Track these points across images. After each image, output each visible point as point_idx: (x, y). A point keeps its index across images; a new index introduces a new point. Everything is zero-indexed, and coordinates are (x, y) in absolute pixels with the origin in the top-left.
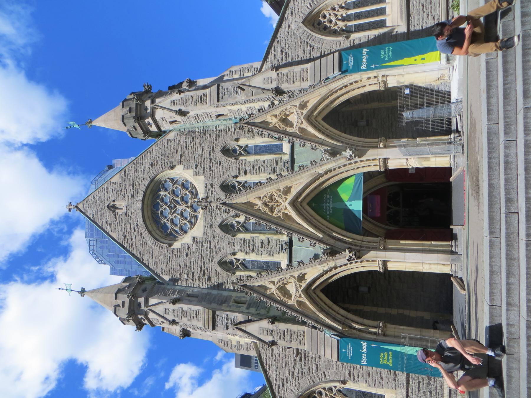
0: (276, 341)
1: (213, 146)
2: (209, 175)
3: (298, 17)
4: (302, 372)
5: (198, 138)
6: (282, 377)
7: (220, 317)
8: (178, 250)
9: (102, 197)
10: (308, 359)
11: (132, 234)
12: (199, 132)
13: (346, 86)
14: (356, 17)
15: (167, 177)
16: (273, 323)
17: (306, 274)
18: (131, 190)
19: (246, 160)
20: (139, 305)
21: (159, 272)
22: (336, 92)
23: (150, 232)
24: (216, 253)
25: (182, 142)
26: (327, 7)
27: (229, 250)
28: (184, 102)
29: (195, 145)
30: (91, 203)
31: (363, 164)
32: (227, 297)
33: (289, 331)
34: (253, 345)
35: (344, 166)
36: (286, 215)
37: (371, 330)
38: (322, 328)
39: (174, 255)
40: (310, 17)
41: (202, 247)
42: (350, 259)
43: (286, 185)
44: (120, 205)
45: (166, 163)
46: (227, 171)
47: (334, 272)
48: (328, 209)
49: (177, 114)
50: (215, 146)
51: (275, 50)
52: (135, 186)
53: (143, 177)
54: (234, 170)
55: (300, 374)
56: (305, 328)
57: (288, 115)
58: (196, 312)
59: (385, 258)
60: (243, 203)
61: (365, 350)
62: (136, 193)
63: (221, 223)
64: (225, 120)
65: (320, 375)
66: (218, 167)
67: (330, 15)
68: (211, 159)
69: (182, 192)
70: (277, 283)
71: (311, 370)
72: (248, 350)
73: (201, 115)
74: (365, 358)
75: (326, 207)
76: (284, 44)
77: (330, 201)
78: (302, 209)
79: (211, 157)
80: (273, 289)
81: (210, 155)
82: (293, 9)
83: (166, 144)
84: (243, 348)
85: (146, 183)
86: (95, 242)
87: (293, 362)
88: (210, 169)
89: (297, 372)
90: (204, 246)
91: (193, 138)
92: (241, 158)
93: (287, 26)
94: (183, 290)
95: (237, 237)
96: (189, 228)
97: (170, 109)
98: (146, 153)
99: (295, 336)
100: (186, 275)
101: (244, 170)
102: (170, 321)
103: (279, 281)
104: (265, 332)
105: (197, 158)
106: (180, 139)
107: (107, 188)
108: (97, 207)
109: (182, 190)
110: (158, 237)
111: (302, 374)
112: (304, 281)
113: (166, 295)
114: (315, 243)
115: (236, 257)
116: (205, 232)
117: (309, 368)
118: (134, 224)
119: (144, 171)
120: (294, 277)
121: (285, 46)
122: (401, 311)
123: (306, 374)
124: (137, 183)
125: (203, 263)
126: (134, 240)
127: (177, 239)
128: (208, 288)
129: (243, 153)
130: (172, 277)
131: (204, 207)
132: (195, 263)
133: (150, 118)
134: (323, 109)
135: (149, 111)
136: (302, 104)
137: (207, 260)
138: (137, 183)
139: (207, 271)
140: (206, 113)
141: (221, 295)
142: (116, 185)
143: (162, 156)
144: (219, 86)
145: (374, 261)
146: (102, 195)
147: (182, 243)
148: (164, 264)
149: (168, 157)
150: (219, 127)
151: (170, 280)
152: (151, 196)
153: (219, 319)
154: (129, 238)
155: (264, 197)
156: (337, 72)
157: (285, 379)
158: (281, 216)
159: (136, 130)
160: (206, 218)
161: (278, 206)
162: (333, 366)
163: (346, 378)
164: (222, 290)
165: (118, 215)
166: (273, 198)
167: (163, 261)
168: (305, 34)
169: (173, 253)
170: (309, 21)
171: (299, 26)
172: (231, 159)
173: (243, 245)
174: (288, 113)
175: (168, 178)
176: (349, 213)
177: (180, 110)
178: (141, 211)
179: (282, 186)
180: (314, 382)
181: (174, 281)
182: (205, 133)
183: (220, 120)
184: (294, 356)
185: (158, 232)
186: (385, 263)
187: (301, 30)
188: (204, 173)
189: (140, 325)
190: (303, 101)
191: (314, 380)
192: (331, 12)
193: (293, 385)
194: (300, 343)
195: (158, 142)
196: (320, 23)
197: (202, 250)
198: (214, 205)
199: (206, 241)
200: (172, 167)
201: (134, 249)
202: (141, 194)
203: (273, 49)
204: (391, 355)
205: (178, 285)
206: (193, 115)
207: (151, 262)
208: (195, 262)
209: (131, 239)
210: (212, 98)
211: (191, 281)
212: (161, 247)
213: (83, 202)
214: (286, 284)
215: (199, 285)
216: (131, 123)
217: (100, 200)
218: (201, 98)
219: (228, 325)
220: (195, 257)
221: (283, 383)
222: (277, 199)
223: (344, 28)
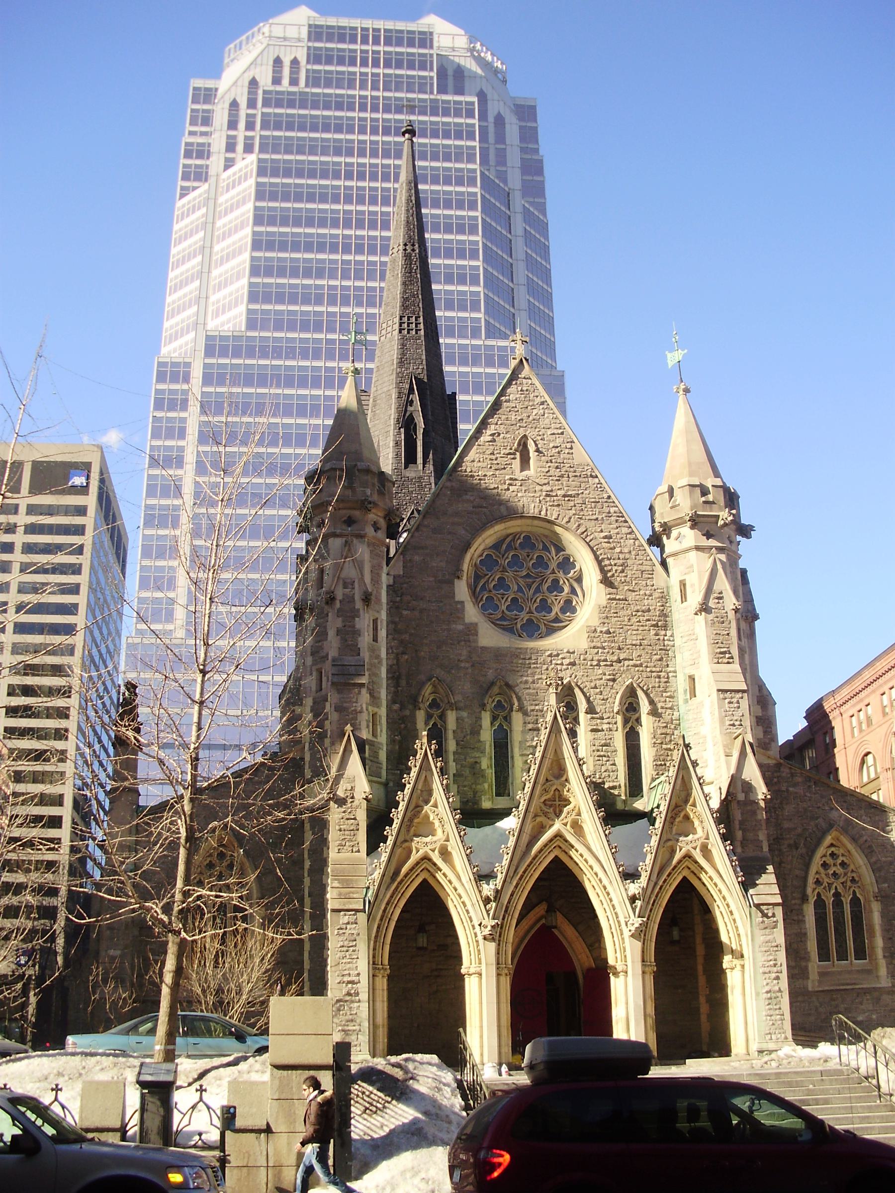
32: (379, 698)
126: (465, 497)
138: (572, 504)
140: (699, 656)
144: (743, 691)
147: (466, 604)
185: (482, 548)
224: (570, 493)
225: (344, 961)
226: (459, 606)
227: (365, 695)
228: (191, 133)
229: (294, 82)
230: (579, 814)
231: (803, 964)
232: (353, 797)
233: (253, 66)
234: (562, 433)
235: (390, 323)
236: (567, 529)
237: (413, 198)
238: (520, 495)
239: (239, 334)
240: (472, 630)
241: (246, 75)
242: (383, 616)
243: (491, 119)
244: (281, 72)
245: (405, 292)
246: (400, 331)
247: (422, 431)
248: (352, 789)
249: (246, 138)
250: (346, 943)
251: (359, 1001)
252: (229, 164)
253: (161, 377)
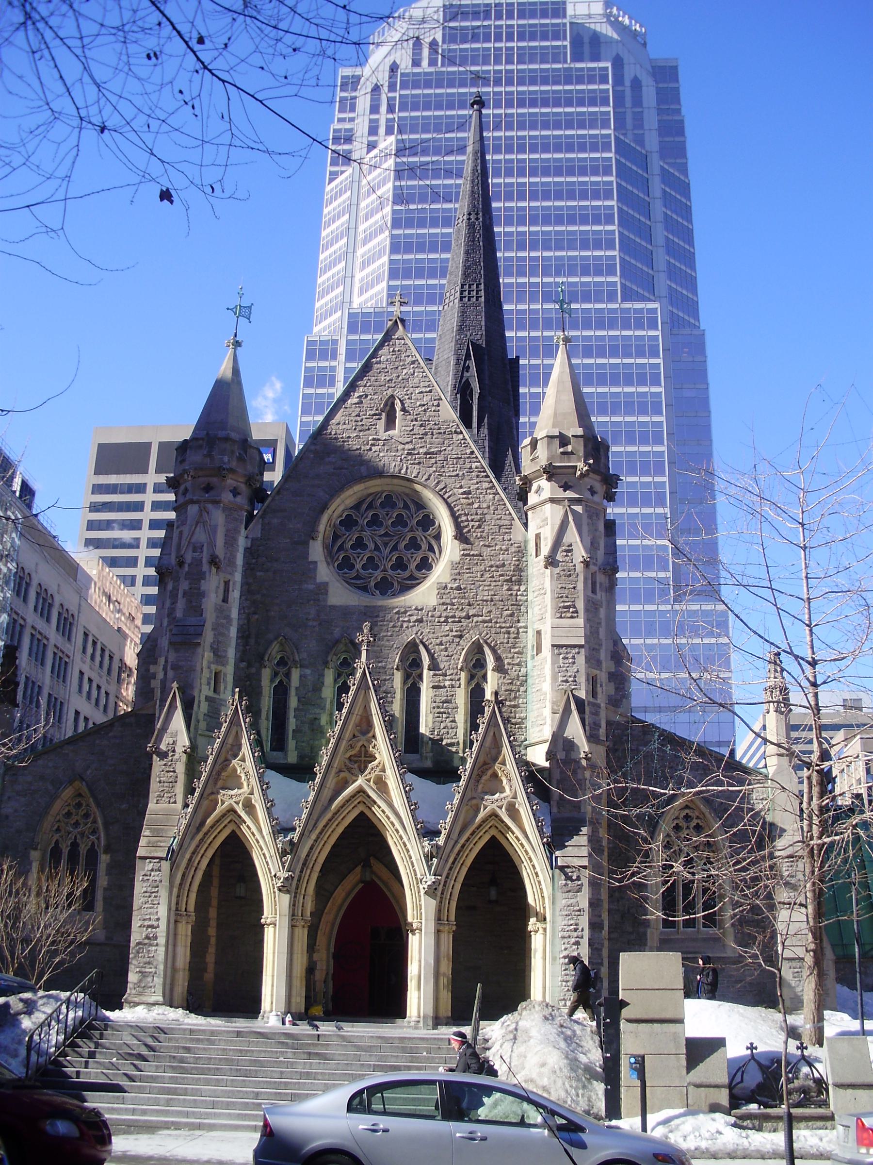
19: (459, 687)
32: (225, 657)
64: (533, 646)
78: (353, 805)
122: (213, 941)
126: (327, 460)
138: (433, 461)
142: (432, 414)
144: (581, 646)
159: (532, 460)
185: (341, 508)
188: (443, 604)
224: (432, 450)
225: (146, 906)
226: (311, 566)
227: (208, 655)
228: (340, 120)
229: (432, 62)
230: (384, 770)
231: (641, 930)
232: (174, 751)
233: (393, 51)
234: (430, 391)
235: (453, 291)
236: (425, 486)
237: (479, 168)
238: (381, 454)
239: (381, 310)
240: (323, 588)
241: (387, 60)
242: (238, 577)
243: (627, 83)
244: (420, 54)
245: (467, 260)
246: (461, 299)
247: (477, 395)
248: (174, 743)
249: (388, 120)
250: (149, 889)
251: (157, 945)
252: (371, 146)
253: (310, 356)
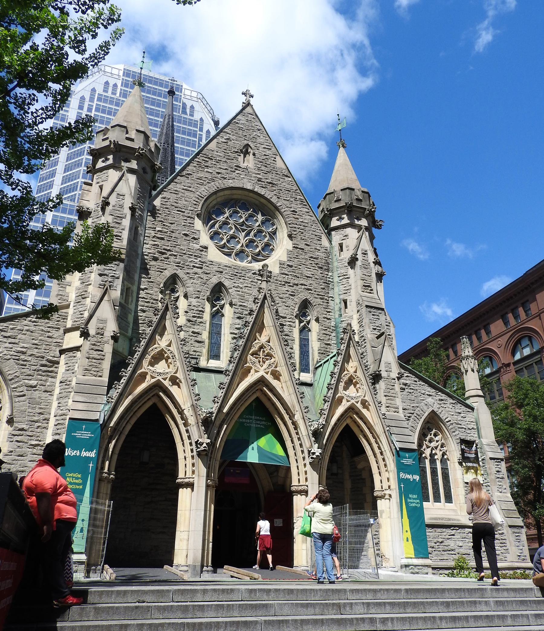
0: (89, 338)
1: (311, 290)
2: (280, 279)
3: (438, 406)
4: (26, 365)
5: (321, 273)
6: (18, 337)
7: (116, 267)
8: (193, 225)
9: (259, 140)
10: (43, 376)
11: (214, 169)
12: (328, 276)
13: (382, 453)
14: (433, 469)
15: (279, 227)
16: (113, 337)
17: (179, 387)
18: (266, 179)
19: (295, 327)
20: (127, 161)
21: (165, 194)
22: (377, 442)
23: (215, 193)
24: (188, 273)
25: (318, 254)
26: (445, 439)
27: (190, 290)
28: (365, 266)
29: (313, 268)
30: (253, 125)
31: (301, 467)
32: (133, 278)
33: (102, 357)
34: (65, 303)
35: (301, 445)
36: (248, 370)
37: (107, 463)
38: (113, 401)
39: (186, 218)
40: (437, 420)
41: (195, 256)
42: (199, 444)
43: (282, 375)
44: (248, 161)
45: (295, 229)
46: (284, 302)
47: (180, 422)
48: (248, 421)
49: (353, 256)
50: (312, 292)
51: (407, 376)
52: (271, 185)
53: (281, 198)
54: (284, 311)
55: (22, 363)
56: (105, 379)
57: (355, 386)
58: (120, 237)
59: (198, 487)
60: (263, 320)
61: (84, 454)
62: (263, 185)
63: (224, 286)
64: (340, 309)
65: (21, 389)
66: (288, 293)
67: (437, 441)
68: (297, 285)
69: (260, 243)
70: (169, 350)
71: (27, 377)
72: (58, 295)
73: (349, 283)
74: (73, 454)
75: (251, 419)
76: (413, 388)
77: (258, 424)
79: (300, 286)
80: (162, 343)
81: (302, 285)
82: (446, 402)
83: (316, 234)
84: (61, 289)
85: (274, 200)
86: (117, 77)
87: (40, 355)
88: (287, 282)
89: (26, 359)
90: (197, 259)
91: (321, 268)
92: (297, 321)
93: (430, 393)
94: (143, 222)
95: (207, 303)
96: (217, 243)
97: (358, 247)
98: (308, 207)
99: (95, 364)
100: (161, 229)
101: (284, 323)
102: (108, 198)
103: (171, 353)
104: (101, 326)
105: (300, 268)
106: (321, 251)
107: (270, 149)
108: (247, 131)
109: (262, 242)
110: (208, 202)
111: (22, 365)
112: (171, 384)
113: (138, 199)
114: (218, 402)
115: (182, 298)
116: (213, 264)
117: (31, 375)
118: (225, 174)
119: (288, 200)
120: (176, 373)
121: (410, 389)
123: (23, 370)
124: (274, 188)
125: (176, 254)
126: (206, 170)
127: (205, 225)
128: (143, 255)
129: (302, 324)
130: (158, 210)
131: (261, 273)
132: (175, 243)
133: (349, 222)
134: (359, 426)
135: (356, 222)
136: (367, 403)
137: (179, 260)
138: (274, 188)
139: (165, 258)
141: (136, 272)
142: (272, 161)
143: (304, 226)
145: (193, 472)
146: (261, 140)
147: (201, 232)
148: (176, 202)
149: (302, 233)
150: (331, 300)
151: (154, 206)
152: (257, 202)
153: (113, 265)
154: (209, 164)
155: (269, 347)
156: (398, 445)
157: (16, 341)
158: (248, 365)
160: (229, 267)
161: (259, 362)
162: (33, 408)
163: (16, 425)
164: (141, 273)
165: (237, 156)
166: (267, 357)
167: (180, 202)
168: (422, 412)
169: (189, 217)
170: (433, 418)
171: (430, 406)
172: (296, 309)
173: (196, 309)
174: (358, 386)
175: (277, 228)
176: (244, 445)
177: (357, 259)
178: (241, 186)
179: (282, 369)
180: (11, 380)
181: (153, 212)
182: (327, 283)
183: (340, 303)
184: (49, 358)
185: (214, 202)
186: (191, 485)
187: (425, 408)
188: (283, 274)
189: (96, 154)
190: (370, 405)
191: (13, 381)
192: (440, 443)
193: (7, 350)
194: (86, 370)
195: (319, 224)
196: (430, 430)
197: (192, 255)
198: (264, 285)
199: (202, 262)
200: (290, 236)
201: (195, 167)
202: (262, 192)
203: (409, 375)
204: (78, 487)
205: (147, 215)
206: (348, 273)
207: (178, 186)
208: (177, 244)
209: (207, 166)
210: (369, 300)
211: (153, 235)
212: (196, 203)
213: (254, 114)
214: (167, 361)
215: (148, 244)
216: (345, 199)
217: (256, 137)
218: (369, 286)
219: (105, 276)
220: (184, 244)
221: (9, 337)
222: (267, 362)
223: (423, 455)
229: (114, 93)
